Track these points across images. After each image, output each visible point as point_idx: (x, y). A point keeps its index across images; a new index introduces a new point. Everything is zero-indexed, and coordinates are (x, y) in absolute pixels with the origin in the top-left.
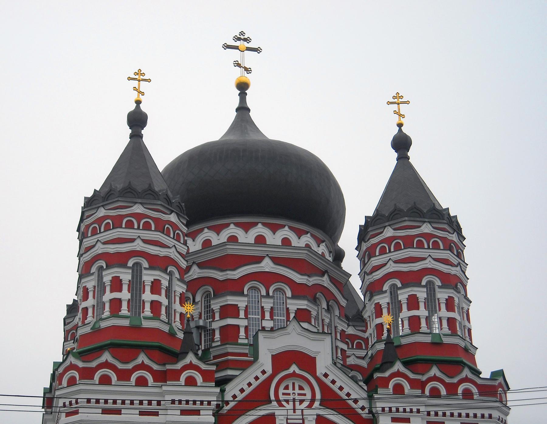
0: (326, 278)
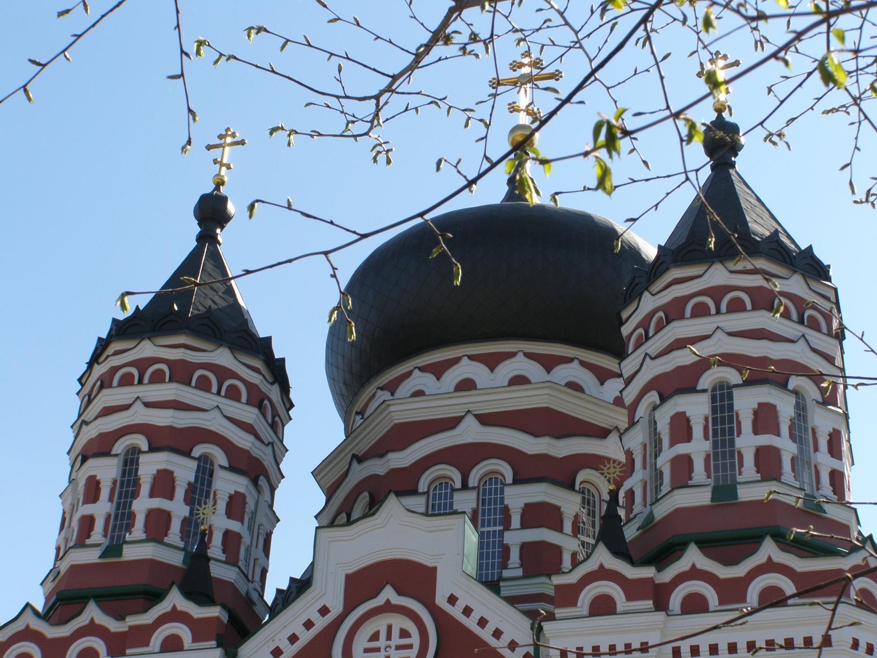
0: (613, 437)
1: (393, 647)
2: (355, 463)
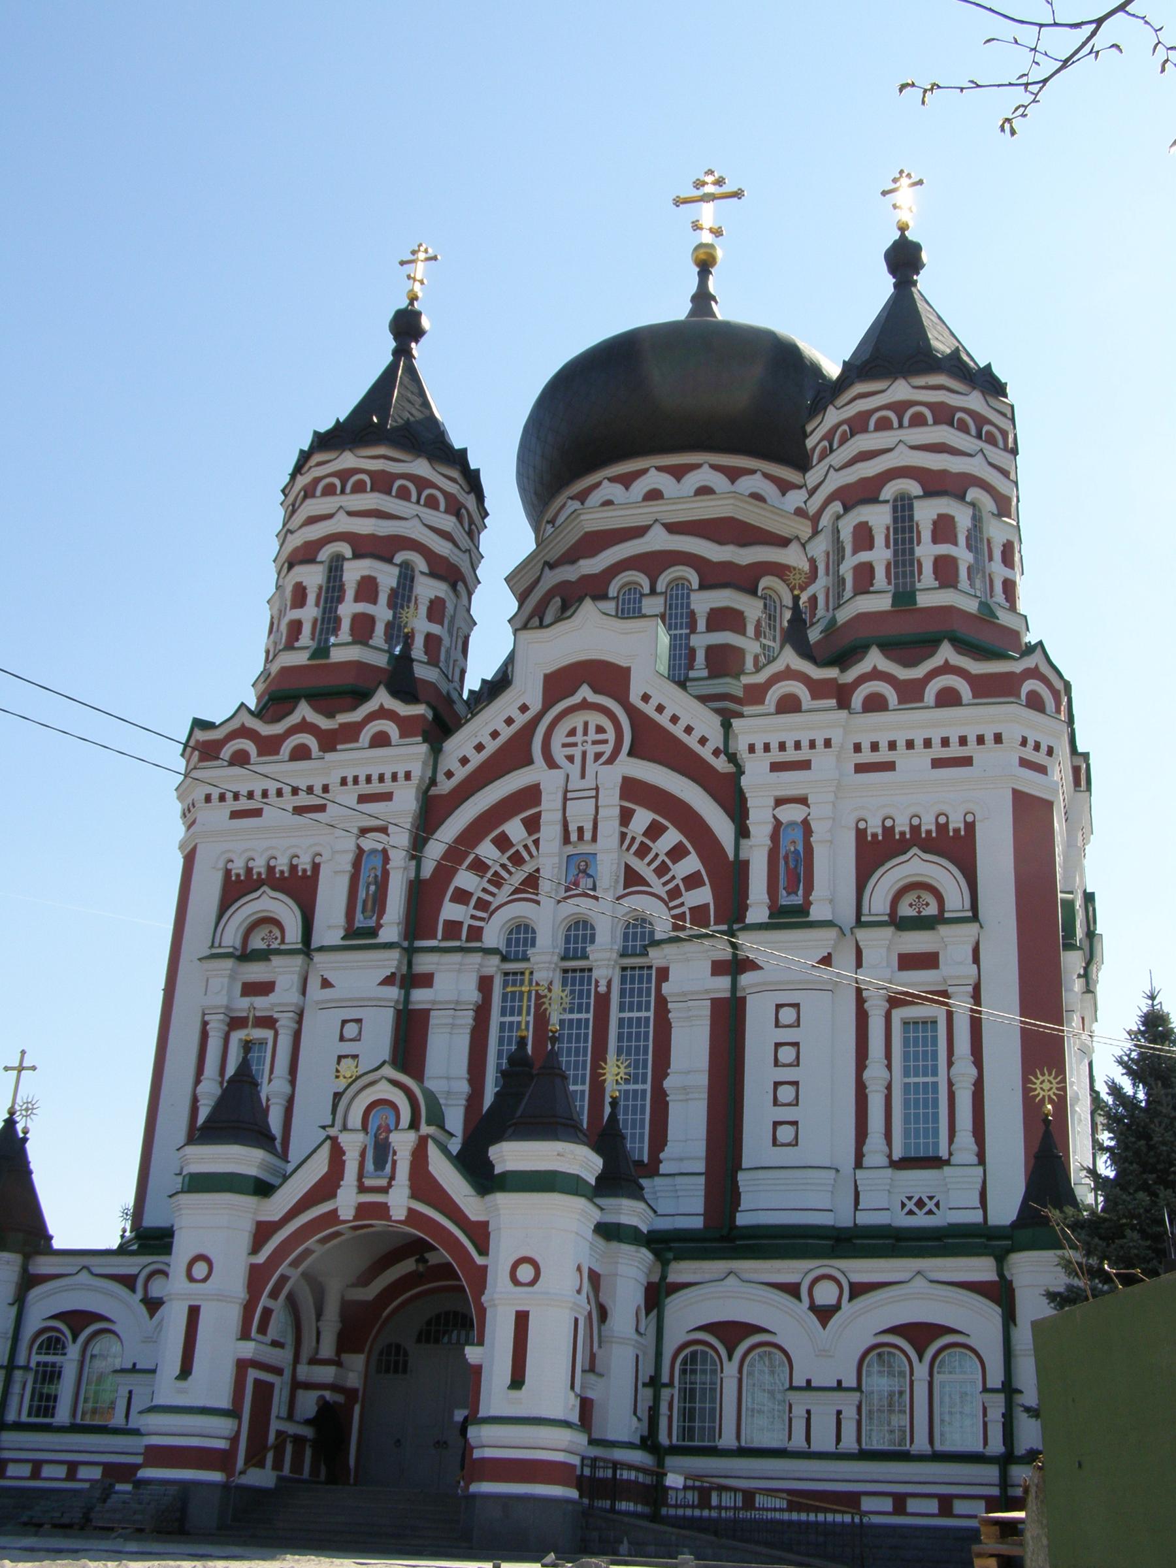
0: (794, 547)
1: (590, 742)
2: (547, 569)
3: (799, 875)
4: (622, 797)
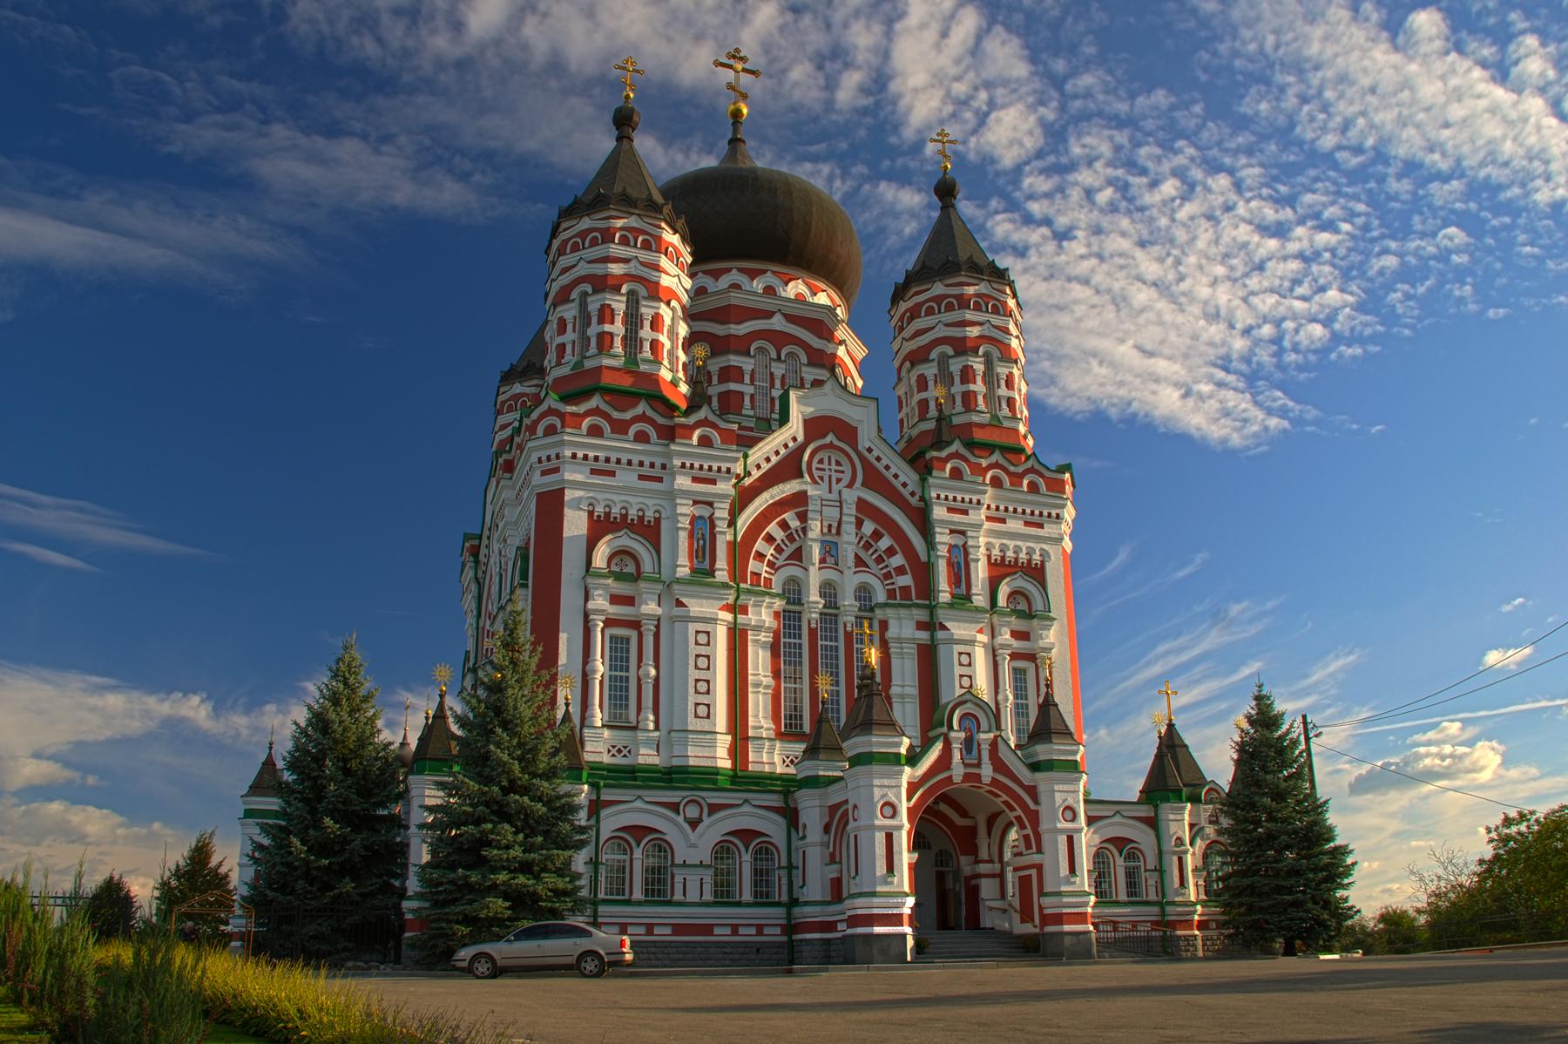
3: (960, 577)
4: (858, 509)
